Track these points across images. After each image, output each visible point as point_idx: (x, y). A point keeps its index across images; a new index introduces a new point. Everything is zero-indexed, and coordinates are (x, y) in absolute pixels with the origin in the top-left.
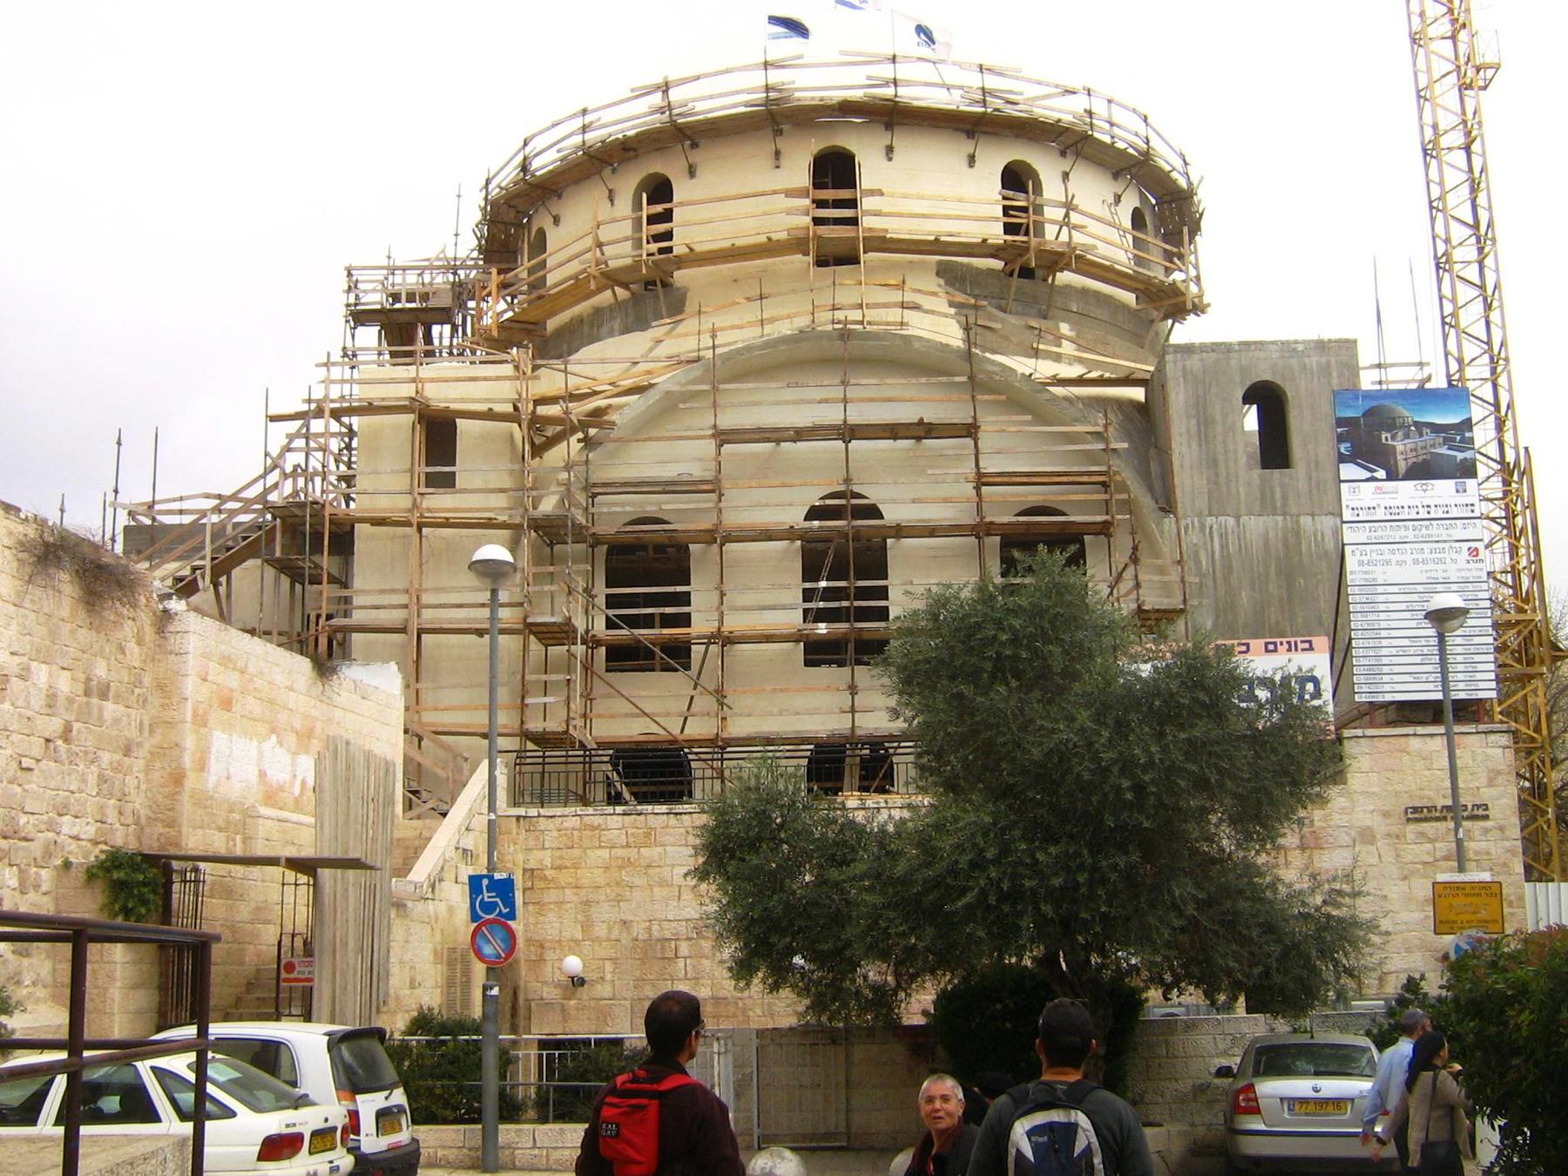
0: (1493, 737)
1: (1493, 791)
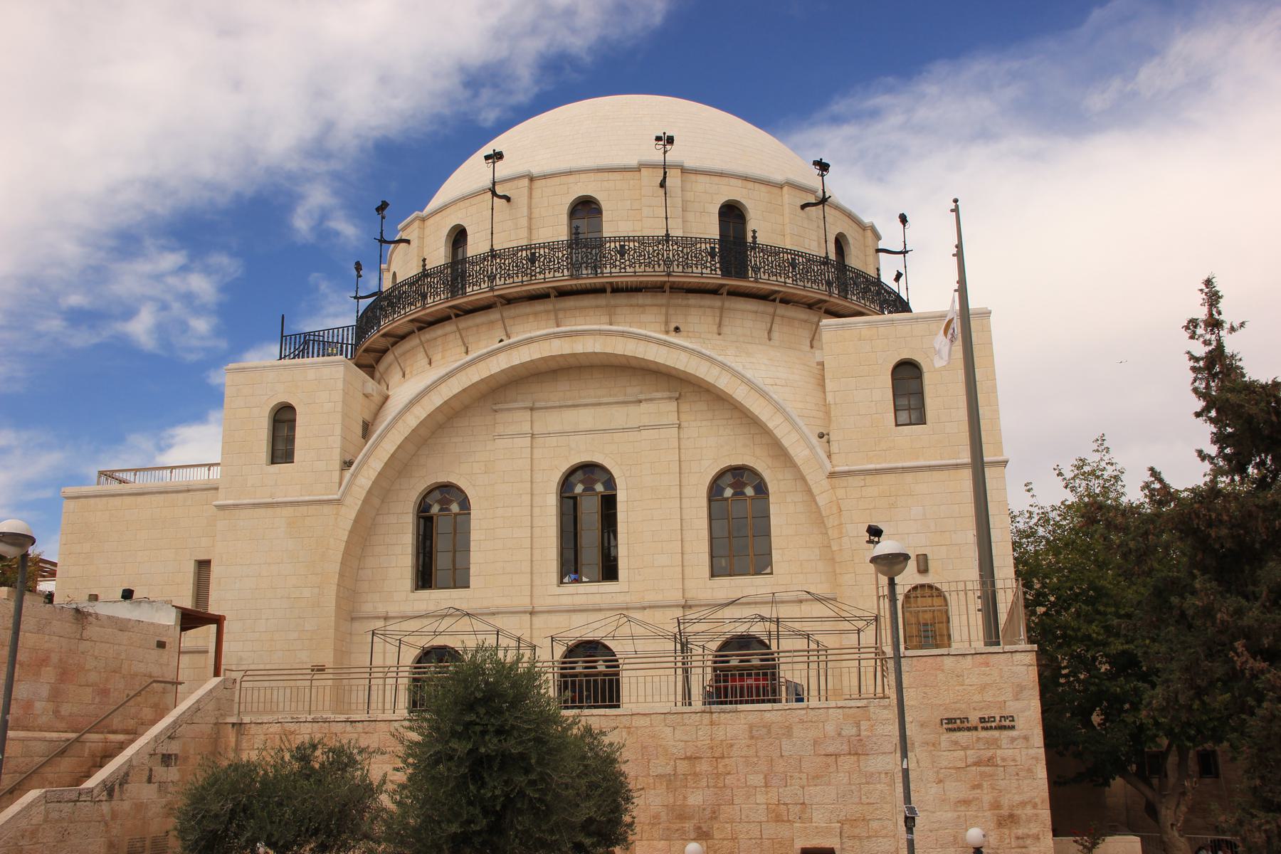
0: (1018, 656)
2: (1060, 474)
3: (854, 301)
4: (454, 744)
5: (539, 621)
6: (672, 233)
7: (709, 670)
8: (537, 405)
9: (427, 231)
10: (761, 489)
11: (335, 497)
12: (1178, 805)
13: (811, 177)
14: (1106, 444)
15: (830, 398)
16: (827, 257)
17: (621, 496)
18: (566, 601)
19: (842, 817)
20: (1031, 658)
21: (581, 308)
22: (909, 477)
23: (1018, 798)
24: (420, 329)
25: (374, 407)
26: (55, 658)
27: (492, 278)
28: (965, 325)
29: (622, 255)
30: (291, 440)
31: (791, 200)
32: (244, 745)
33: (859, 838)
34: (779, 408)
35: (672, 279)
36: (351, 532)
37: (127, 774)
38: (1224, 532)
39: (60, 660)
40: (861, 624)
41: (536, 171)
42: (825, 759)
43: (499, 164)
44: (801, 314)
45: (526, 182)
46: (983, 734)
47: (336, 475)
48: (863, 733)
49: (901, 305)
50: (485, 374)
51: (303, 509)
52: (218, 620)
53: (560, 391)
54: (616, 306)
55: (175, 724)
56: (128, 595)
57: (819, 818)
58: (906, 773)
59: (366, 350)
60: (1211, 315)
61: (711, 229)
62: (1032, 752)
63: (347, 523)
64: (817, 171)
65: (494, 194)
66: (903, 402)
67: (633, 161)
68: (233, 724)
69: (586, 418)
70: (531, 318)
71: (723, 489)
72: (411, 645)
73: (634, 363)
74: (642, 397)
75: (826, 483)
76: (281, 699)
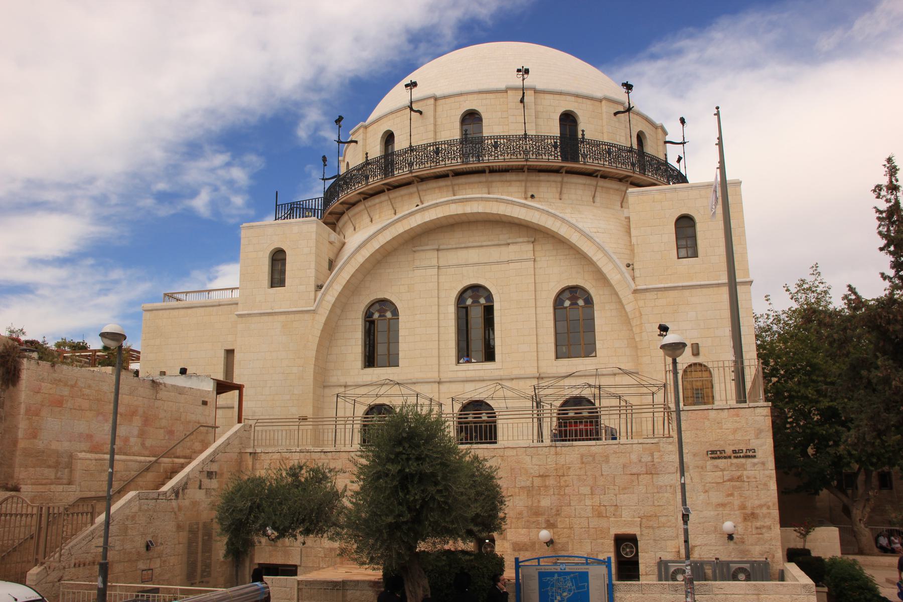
0: (758, 410)
1: (759, 442)
2: (788, 290)
3: (650, 176)
4: (389, 466)
5: (444, 387)
6: (528, 133)
7: (555, 419)
8: (441, 247)
9: (368, 135)
10: (589, 301)
11: (312, 308)
12: (864, 507)
13: (620, 94)
14: (819, 270)
15: (634, 240)
16: (631, 147)
17: (497, 307)
18: (462, 375)
19: (642, 513)
20: (767, 411)
21: (469, 183)
22: (687, 292)
23: (757, 502)
24: (365, 199)
25: (335, 250)
26: (141, 411)
27: (411, 164)
28: (724, 189)
30: (283, 272)
31: (607, 109)
32: (258, 466)
33: (653, 528)
34: (600, 248)
35: (529, 163)
36: (322, 331)
37: (186, 483)
38: (898, 327)
39: (144, 412)
40: (654, 389)
41: (438, 93)
42: (630, 477)
43: (414, 90)
44: (615, 185)
45: (432, 101)
46: (735, 461)
47: (312, 294)
48: (656, 460)
49: (682, 179)
50: (407, 228)
51: (292, 316)
52: (240, 388)
53: (457, 238)
54: (492, 182)
55: (215, 453)
56: (183, 371)
57: (626, 515)
58: (683, 486)
59: (330, 213)
60: (891, 182)
61: (554, 129)
62: (767, 472)
63: (320, 326)
64: (624, 90)
65: (411, 109)
66: (683, 242)
67: (503, 86)
68: (251, 453)
69: (473, 255)
70: (437, 191)
71: (563, 302)
72: (362, 404)
73: (504, 219)
74: (509, 241)
75: (631, 297)
76: (280, 438)
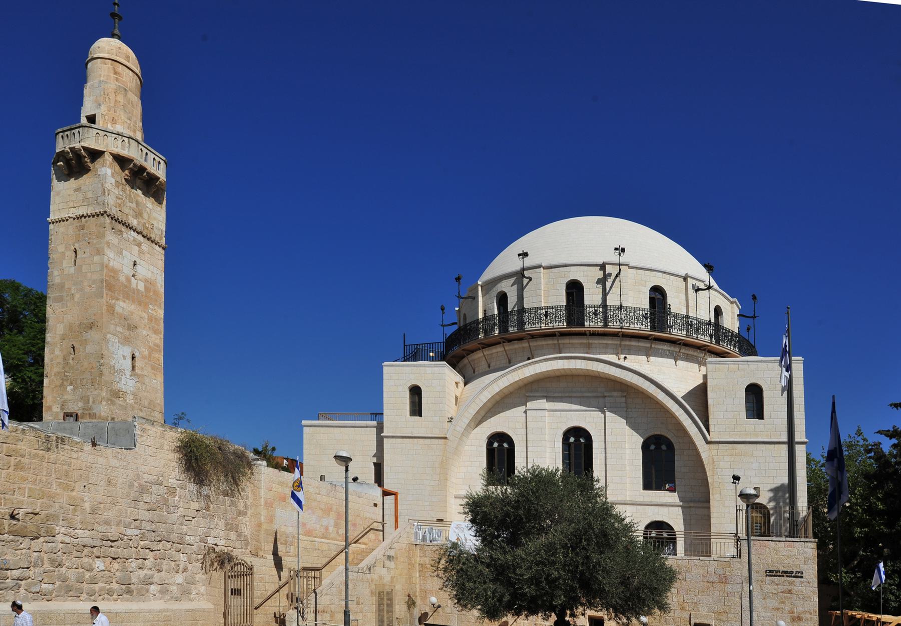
29: (596, 315)
